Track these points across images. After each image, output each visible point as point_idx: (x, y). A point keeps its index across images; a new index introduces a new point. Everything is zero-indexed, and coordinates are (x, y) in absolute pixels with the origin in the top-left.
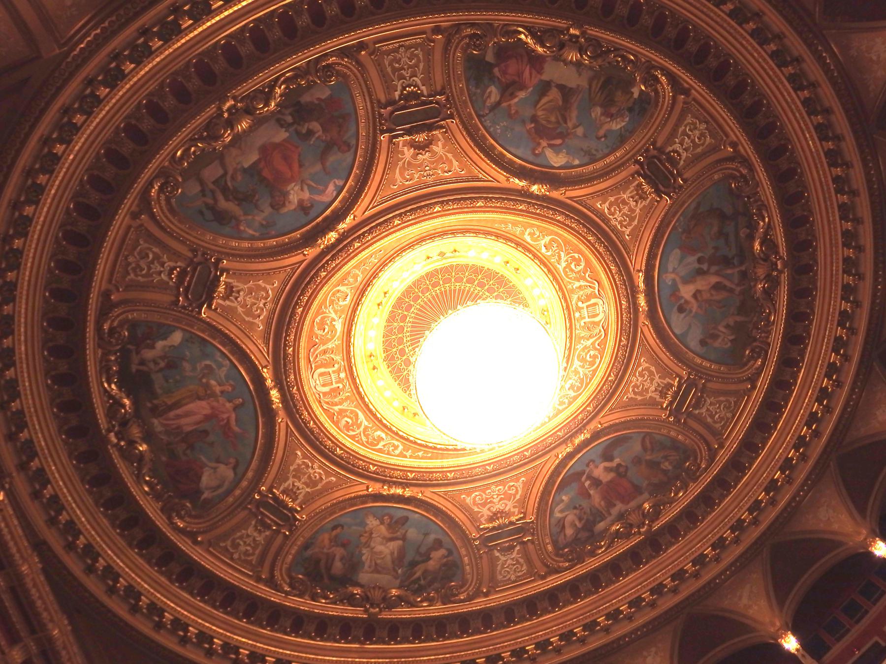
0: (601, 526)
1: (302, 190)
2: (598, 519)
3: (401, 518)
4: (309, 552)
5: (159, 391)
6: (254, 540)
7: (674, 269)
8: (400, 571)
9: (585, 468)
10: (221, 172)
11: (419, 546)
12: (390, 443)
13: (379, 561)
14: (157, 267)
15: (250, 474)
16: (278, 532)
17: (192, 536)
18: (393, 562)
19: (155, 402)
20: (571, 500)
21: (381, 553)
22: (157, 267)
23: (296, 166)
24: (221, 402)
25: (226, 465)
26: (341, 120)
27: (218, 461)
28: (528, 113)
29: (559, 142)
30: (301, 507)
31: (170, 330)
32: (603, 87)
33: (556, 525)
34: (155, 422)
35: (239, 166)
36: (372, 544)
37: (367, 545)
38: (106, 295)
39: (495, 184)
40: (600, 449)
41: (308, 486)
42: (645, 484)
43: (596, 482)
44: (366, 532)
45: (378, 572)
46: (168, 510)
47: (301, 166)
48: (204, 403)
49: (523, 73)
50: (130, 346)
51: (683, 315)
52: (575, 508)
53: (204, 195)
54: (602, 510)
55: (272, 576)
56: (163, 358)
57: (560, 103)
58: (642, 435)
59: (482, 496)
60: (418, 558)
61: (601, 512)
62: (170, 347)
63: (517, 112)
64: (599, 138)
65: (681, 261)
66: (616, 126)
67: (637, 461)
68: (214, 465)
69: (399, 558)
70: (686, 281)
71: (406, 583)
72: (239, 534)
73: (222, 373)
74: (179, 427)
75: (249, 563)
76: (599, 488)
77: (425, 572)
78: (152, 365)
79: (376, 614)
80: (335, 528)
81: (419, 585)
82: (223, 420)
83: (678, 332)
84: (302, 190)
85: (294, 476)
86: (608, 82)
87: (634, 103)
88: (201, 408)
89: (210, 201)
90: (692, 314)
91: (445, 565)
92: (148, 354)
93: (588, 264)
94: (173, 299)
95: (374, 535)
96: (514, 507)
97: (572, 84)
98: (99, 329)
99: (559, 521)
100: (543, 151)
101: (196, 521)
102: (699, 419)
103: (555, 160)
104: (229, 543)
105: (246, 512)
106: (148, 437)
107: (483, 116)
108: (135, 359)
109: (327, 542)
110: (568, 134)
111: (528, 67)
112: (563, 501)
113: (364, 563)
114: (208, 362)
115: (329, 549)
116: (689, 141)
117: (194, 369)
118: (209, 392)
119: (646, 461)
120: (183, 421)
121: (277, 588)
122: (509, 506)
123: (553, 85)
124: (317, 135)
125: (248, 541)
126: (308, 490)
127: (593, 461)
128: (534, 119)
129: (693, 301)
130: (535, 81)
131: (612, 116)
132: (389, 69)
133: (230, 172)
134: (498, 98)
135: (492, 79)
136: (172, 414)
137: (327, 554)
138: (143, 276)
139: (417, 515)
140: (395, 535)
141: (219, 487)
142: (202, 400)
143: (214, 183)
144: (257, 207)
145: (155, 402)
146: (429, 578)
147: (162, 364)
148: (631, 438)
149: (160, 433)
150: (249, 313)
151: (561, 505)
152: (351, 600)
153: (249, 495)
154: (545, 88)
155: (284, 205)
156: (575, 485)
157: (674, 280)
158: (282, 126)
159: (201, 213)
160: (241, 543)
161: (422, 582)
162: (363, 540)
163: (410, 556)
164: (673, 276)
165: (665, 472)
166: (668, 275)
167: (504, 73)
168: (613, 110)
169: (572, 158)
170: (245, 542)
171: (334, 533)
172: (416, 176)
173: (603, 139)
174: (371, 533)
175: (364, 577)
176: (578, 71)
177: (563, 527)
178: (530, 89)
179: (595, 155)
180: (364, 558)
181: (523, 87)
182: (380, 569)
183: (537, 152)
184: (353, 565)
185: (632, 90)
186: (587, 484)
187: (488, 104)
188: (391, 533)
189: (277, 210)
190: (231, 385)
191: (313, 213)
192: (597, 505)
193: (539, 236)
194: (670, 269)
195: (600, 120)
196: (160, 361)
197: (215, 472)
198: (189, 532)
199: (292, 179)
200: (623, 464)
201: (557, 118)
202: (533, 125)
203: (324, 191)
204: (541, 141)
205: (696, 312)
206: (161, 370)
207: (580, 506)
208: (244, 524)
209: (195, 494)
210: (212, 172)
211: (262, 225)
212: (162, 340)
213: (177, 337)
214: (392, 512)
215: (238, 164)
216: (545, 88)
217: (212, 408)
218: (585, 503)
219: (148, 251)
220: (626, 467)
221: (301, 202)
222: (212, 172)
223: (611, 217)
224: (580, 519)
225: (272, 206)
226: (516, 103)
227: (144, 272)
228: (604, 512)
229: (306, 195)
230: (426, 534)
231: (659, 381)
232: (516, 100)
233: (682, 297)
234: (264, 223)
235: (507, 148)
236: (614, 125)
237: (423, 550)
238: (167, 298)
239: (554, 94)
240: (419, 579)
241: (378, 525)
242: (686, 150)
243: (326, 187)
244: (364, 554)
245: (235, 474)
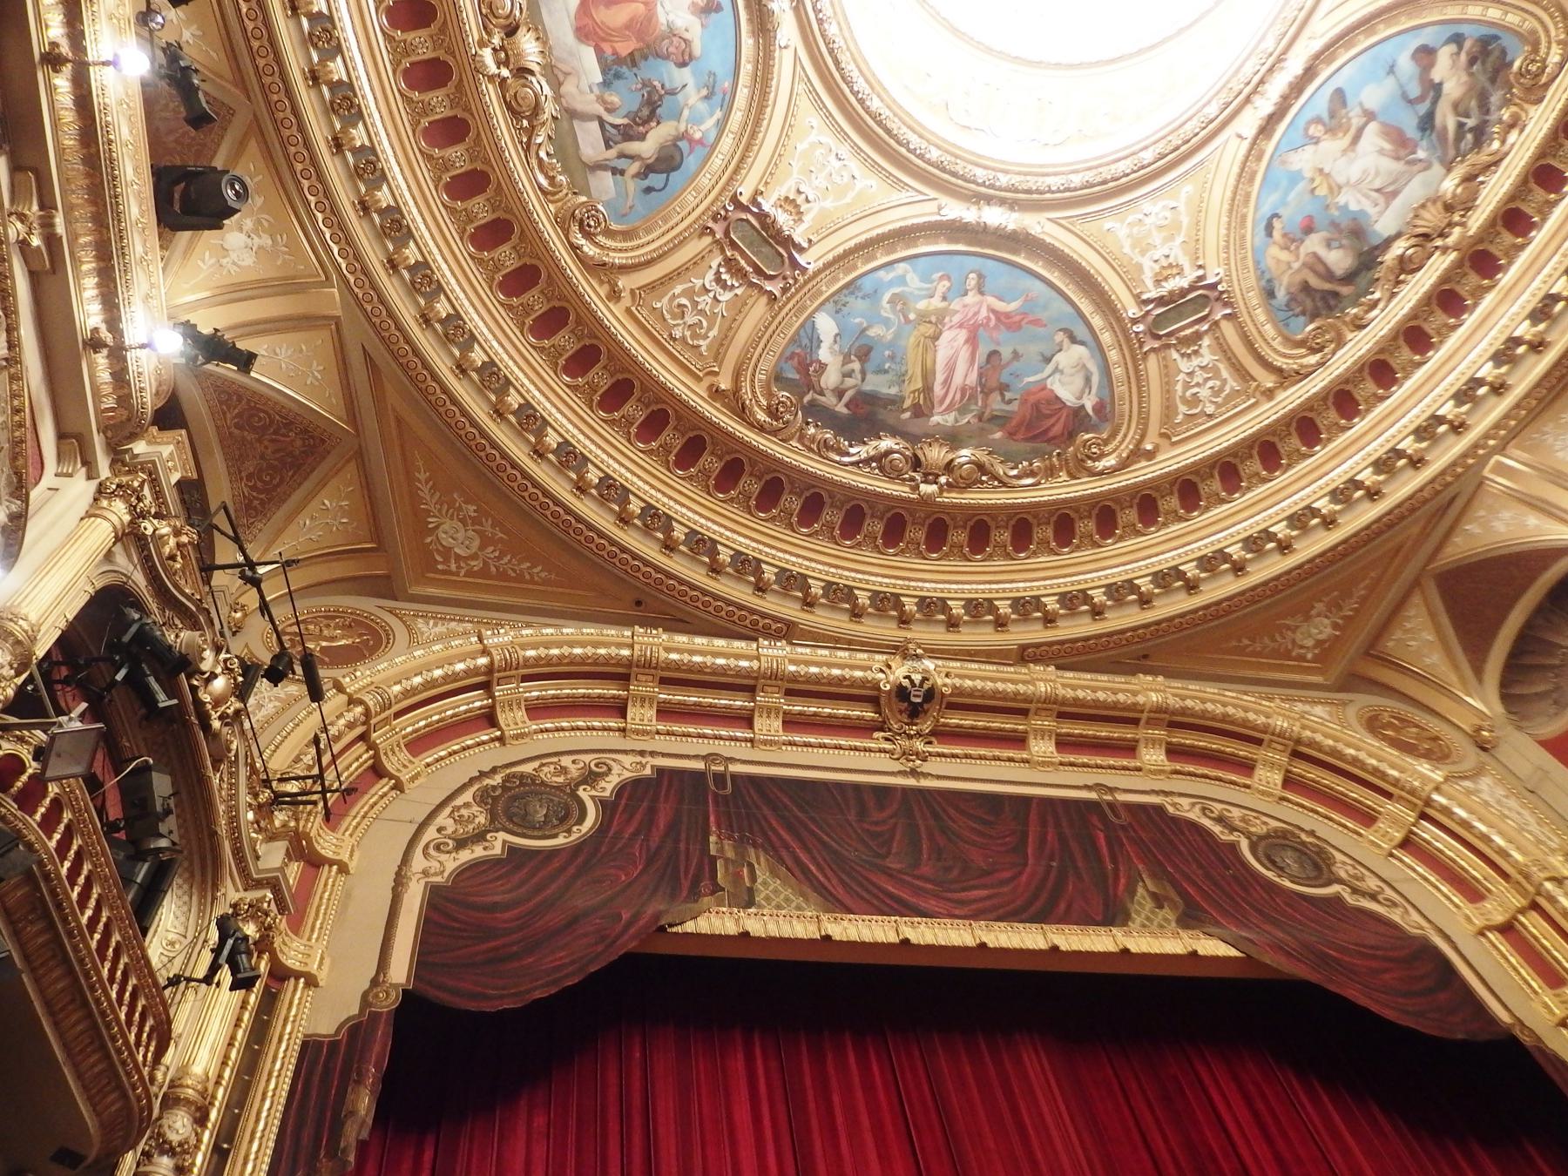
3: (1331, 100)
4: (1281, 295)
5: (894, 391)
6: (1202, 368)
10: (595, 125)
13: (1377, 185)
14: (705, 301)
15: (1097, 321)
16: (1216, 323)
17: (1138, 454)
18: (1398, 159)
19: (907, 403)
21: (1365, 172)
22: (705, 301)
24: (957, 308)
25: (1060, 350)
27: (1048, 360)
30: (1200, 267)
31: (809, 326)
34: (936, 419)
35: (596, 89)
36: (1341, 180)
37: (1336, 189)
38: (716, 393)
41: (1171, 238)
44: (1313, 180)
45: (1395, 194)
46: (1078, 469)
48: (946, 336)
50: (807, 399)
53: (622, 172)
55: (1279, 371)
56: (846, 360)
60: (1423, 108)
62: (835, 342)
68: (1050, 368)
69: (1401, 143)
71: (1452, 152)
72: (1179, 387)
73: (914, 282)
74: (963, 390)
75: (1235, 394)
78: (849, 382)
79: (1463, 237)
80: (1269, 229)
81: (1471, 130)
82: (988, 319)
85: (1143, 253)
88: (951, 344)
89: (635, 167)
92: (830, 379)
94: (764, 300)
95: (1326, 170)
98: (761, 428)
101: (1119, 438)
104: (1183, 409)
105: (1152, 358)
106: (953, 439)
108: (829, 400)
109: (1285, 256)
113: (1362, 212)
114: (887, 297)
117: (886, 322)
118: (933, 319)
120: (958, 380)
121: (1301, 375)
125: (1198, 379)
126: (1179, 240)
133: (600, 110)
136: (938, 390)
137: (1305, 265)
138: (710, 329)
141: (1088, 380)
142: (940, 333)
143: (608, 147)
144: (672, 93)
145: (907, 403)
146: (1473, 103)
147: (856, 366)
149: (957, 421)
152: (1406, 267)
153: (1128, 340)
159: (649, 190)
160: (1195, 390)
161: (1471, 122)
162: (1322, 191)
163: (1409, 122)
170: (1198, 385)
171: (1277, 234)
174: (1321, 170)
175: (1385, 223)
182: (1390, 189)
184: (1355, 231)
189: (691, 57)
190: (941, 278)
196: (850, 366)
197: (1062, 372)
198: (1128, 457)
206: (863, 373)
208: (1168, 373)
209: (1078, 419)
210: (590, 142)
211: (707, 98)
212: (819, 347)
213: (826, 325)
214: (1309, 114)
215: (592, 91)
217: (961, 326)
219: (676, 303)
222: (590, 142)
225: (683, 64)
227: (705, 324)
230: (1391, 70)
234: (704, 92)
237: (1415, 91)
238: (760, 308)
240: (1461, 125)
241: (1315, 152)
245: (1082, 343)
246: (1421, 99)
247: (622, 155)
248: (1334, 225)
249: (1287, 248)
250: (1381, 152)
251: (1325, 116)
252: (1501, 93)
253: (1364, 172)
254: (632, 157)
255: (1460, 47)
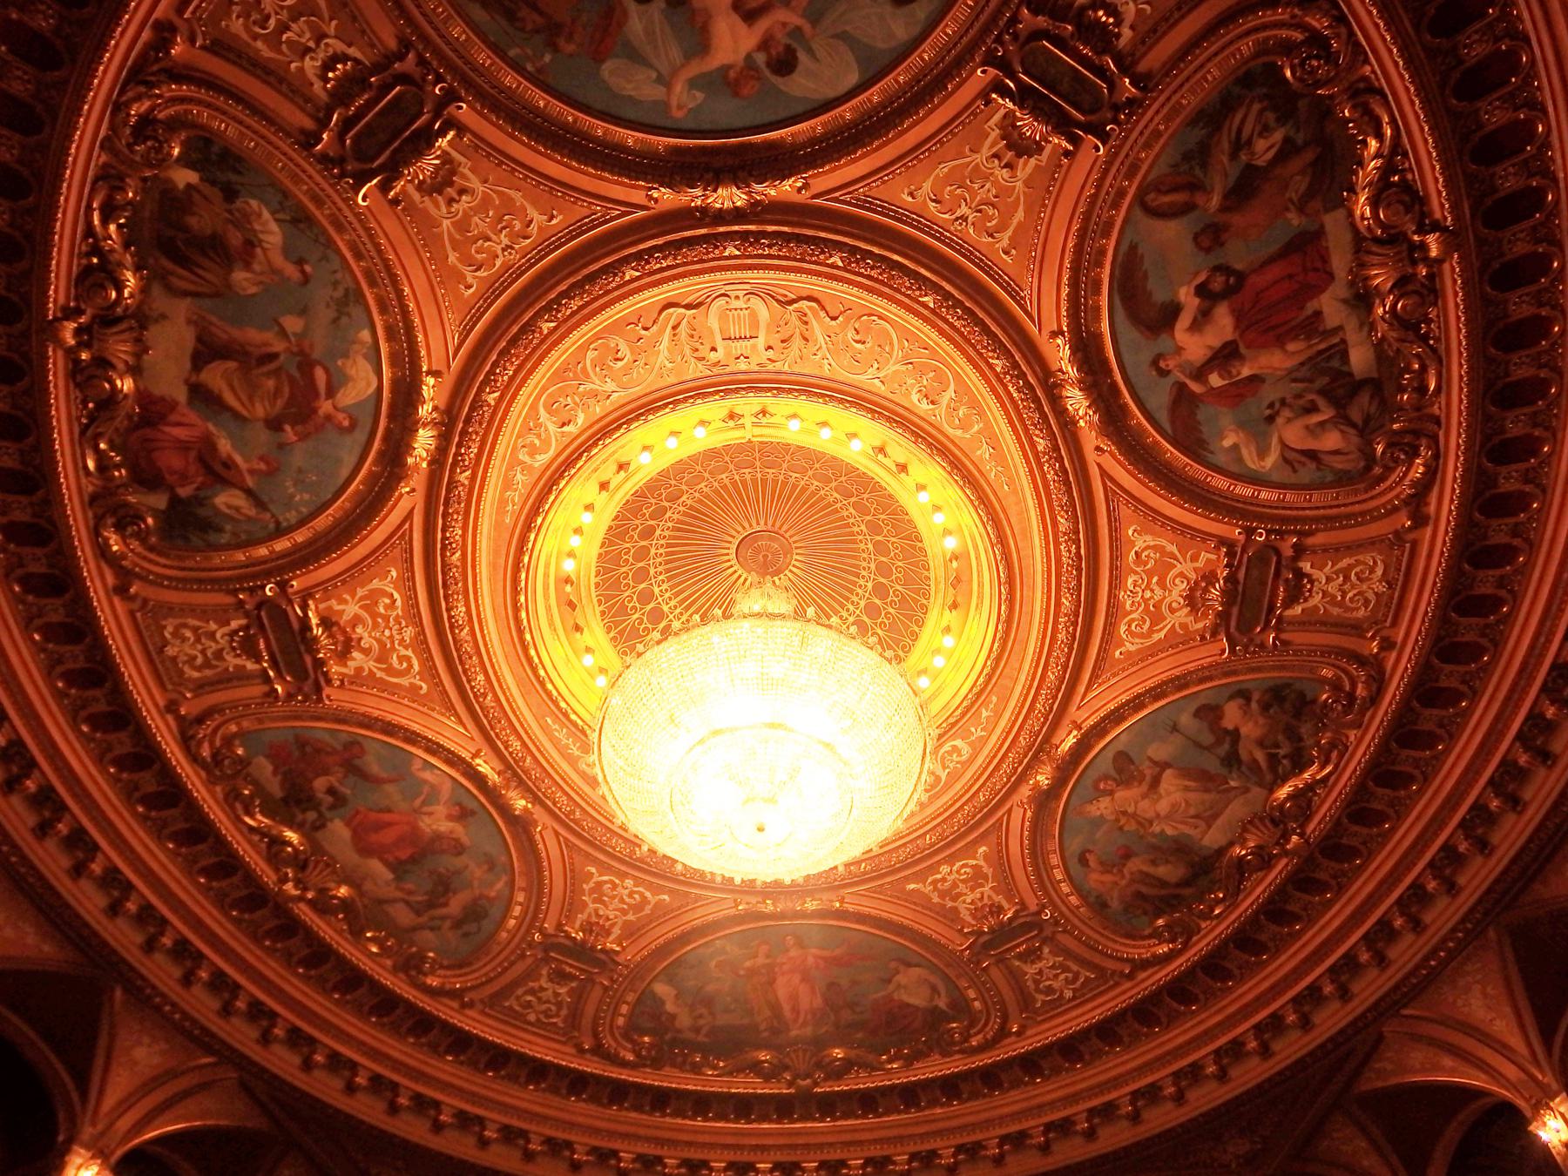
0: (1360, 359)
1: (430, 814)
2: (1335, 363)
4: (1115, 904)
7: (661, 80)
8: (1233, 784)
9: (1170, 380)
11: (1198, 745)
12: (943, 758)
13: (1192, 811)
18: (1207, 790)
20: (1242, 425)
23: (386, 817)
26: (308, 749)
28: (263, 436)
29: (320, 374)
32: (183, 261)
33: (1295, 471)
36: (1150, 814)
39: (418, 519)
40: (1129, 333)
42: (1295, 219)
43: (1225, 356)
44: (1117, 820)
45: (1215, 816)
47: (389, 811)
49: (181, 441)
51: (802, 56)
52: (1271, 419)
53: (439, 928)
54: (1310, 353)
57: (232, 365)
58: (1138, 213)
59: (1133, 620)
61: (1320, 353)
63: (262, 458)
64: (306, 279)
65: (635, 56)
66: (272, 233)
67: (1211, 236)
69: (1204, 778)
70: (701, 43)
71: (1269, 777)
76: (1243, 350)
77: (1261, 743)
78: (701, 1022)
80: (1083, 861)
81: (1285, 757)
83: (853, 79)
84: (430, 814)
86: (169, 248)
87: (213, 183)
89: (448, 923)
90: (807, 28)
91: (1265, 707)
93: (615, 328)
95: (1131, 810)
96: (1195, 558)
97: (189, 336)
98: (632, 1066)
99: (1286, 460)
100: (343, 410)
102: (1151, 33)
103: (363, 384)
107: (278, 523)
110: (302, 353)
111: (167, 429)
112: (1235, 447)
115: (1123, 877)
116: (294, 26)
119: (1223, 209)
122: (1187, 568)
123: (194, 379)
124: (336, 784)
127: (1155, 363)
128: (275, 425)
129: (763, 24)
130: (192, 417)
131: (250, 244)
132: (208, 672)
133: (399, 894)
134: (237, 492)
135: (198, 500)
137: (1132, 881)
139: (1123, 737)
140: (1148, 779)
144: (458, 872)
148: (1133, 248)
150: (638, 908)
151: (1245, 452)
154: (200, 395)
155: (457, 840)
156: (1204, 413)
157: (693, 83)
158: (323, 826)
163: (1212, 764)
164: (678, 88)
165: (1287, 151)
166: (674, 103)
167: (184, 478)
168: (235, 239)
169: (356, 347)
172: (403, 652)
173: (308, 268)
174: (1124, 813)
176: (156, 321)
177: (1312, 455)
178: (211, 427)
179: (347, 290)
180: (1169, 832)
181: (208, 443)
183: (346, 423)
185: (181, 186)
186: (1215, 380)
187: (252, 512)
188: (1140, 783)
191: (472, 805)
192: (1290, 363)
193: (539, 436)
194: (658, 92)
195: (262, 273)
199: (415, 829)
200: (1202, 278)
201: (268, 375)
202: (288, 428)
203: (433, 787)
204: (321, 412)
205: (803, 16)
207: (1271, 406)
214: (1093, 774)
216: (200, 395)
218: (1270, 393)
220: (1217, 269)
221: (450, 818)
223: (498, 263)
224: (1312, 409)
225: (459, 854)
226: (247, 460)
228: (1322, 346)
229: (441, 810)
230: (1175, 728)
231: (986, 151)
232: (238, 459)
233: (749, 57)
234: (486, 867)
235: (340, 481)
236: (270, 238)
237: (1207, 738)
239: (216, 377)
240: (1273, 760)
242: (320, 37)
243: (425, 782)
244: (1163, 831)
246: (1219, 742)
247: (432, 919)
248: (1155, 848)
249: (1110, 872)
250: (1186, 789)
251: (1113, 773)
252: (1309, 725)
253: (1173, 806)
254: (443, 918)
255: (1248, 700)
